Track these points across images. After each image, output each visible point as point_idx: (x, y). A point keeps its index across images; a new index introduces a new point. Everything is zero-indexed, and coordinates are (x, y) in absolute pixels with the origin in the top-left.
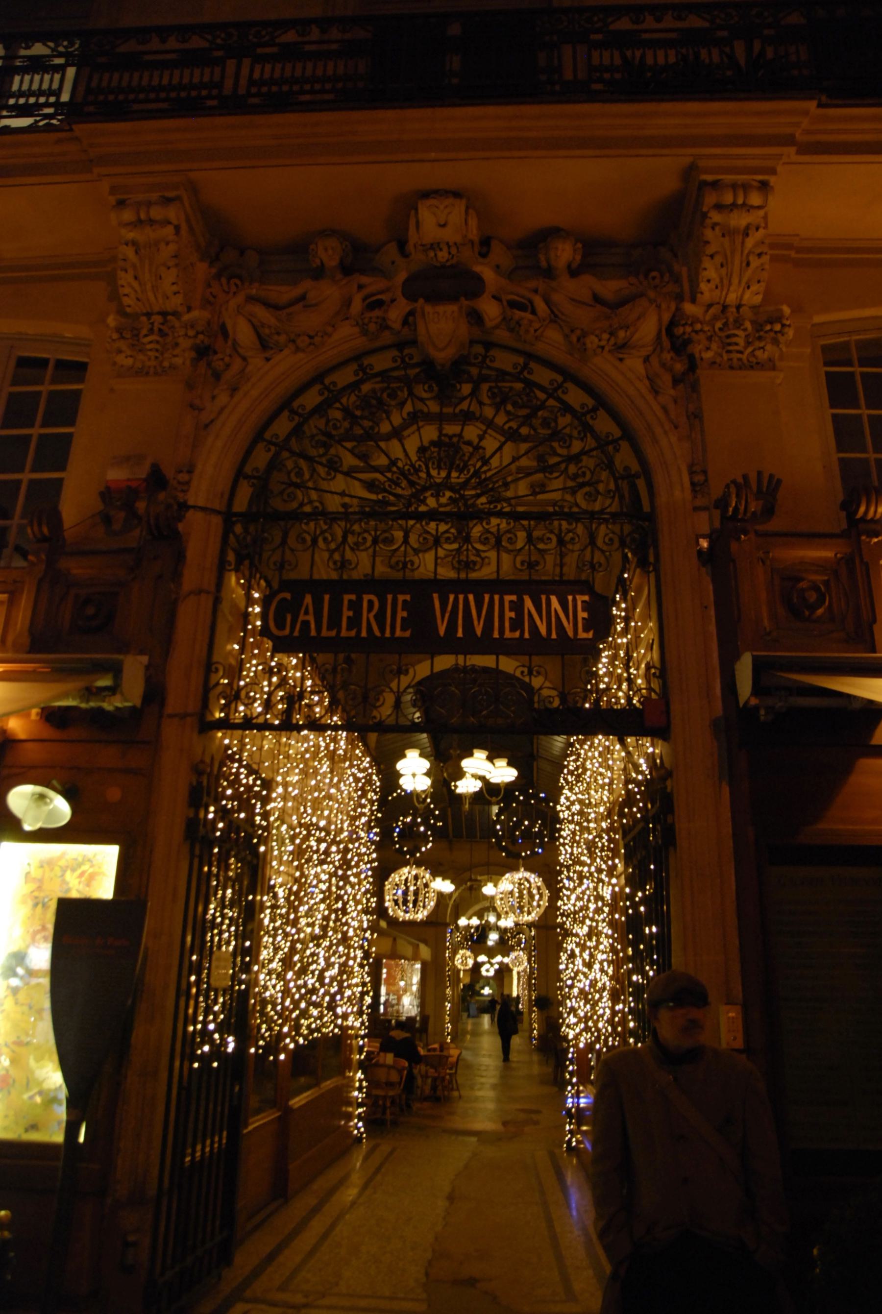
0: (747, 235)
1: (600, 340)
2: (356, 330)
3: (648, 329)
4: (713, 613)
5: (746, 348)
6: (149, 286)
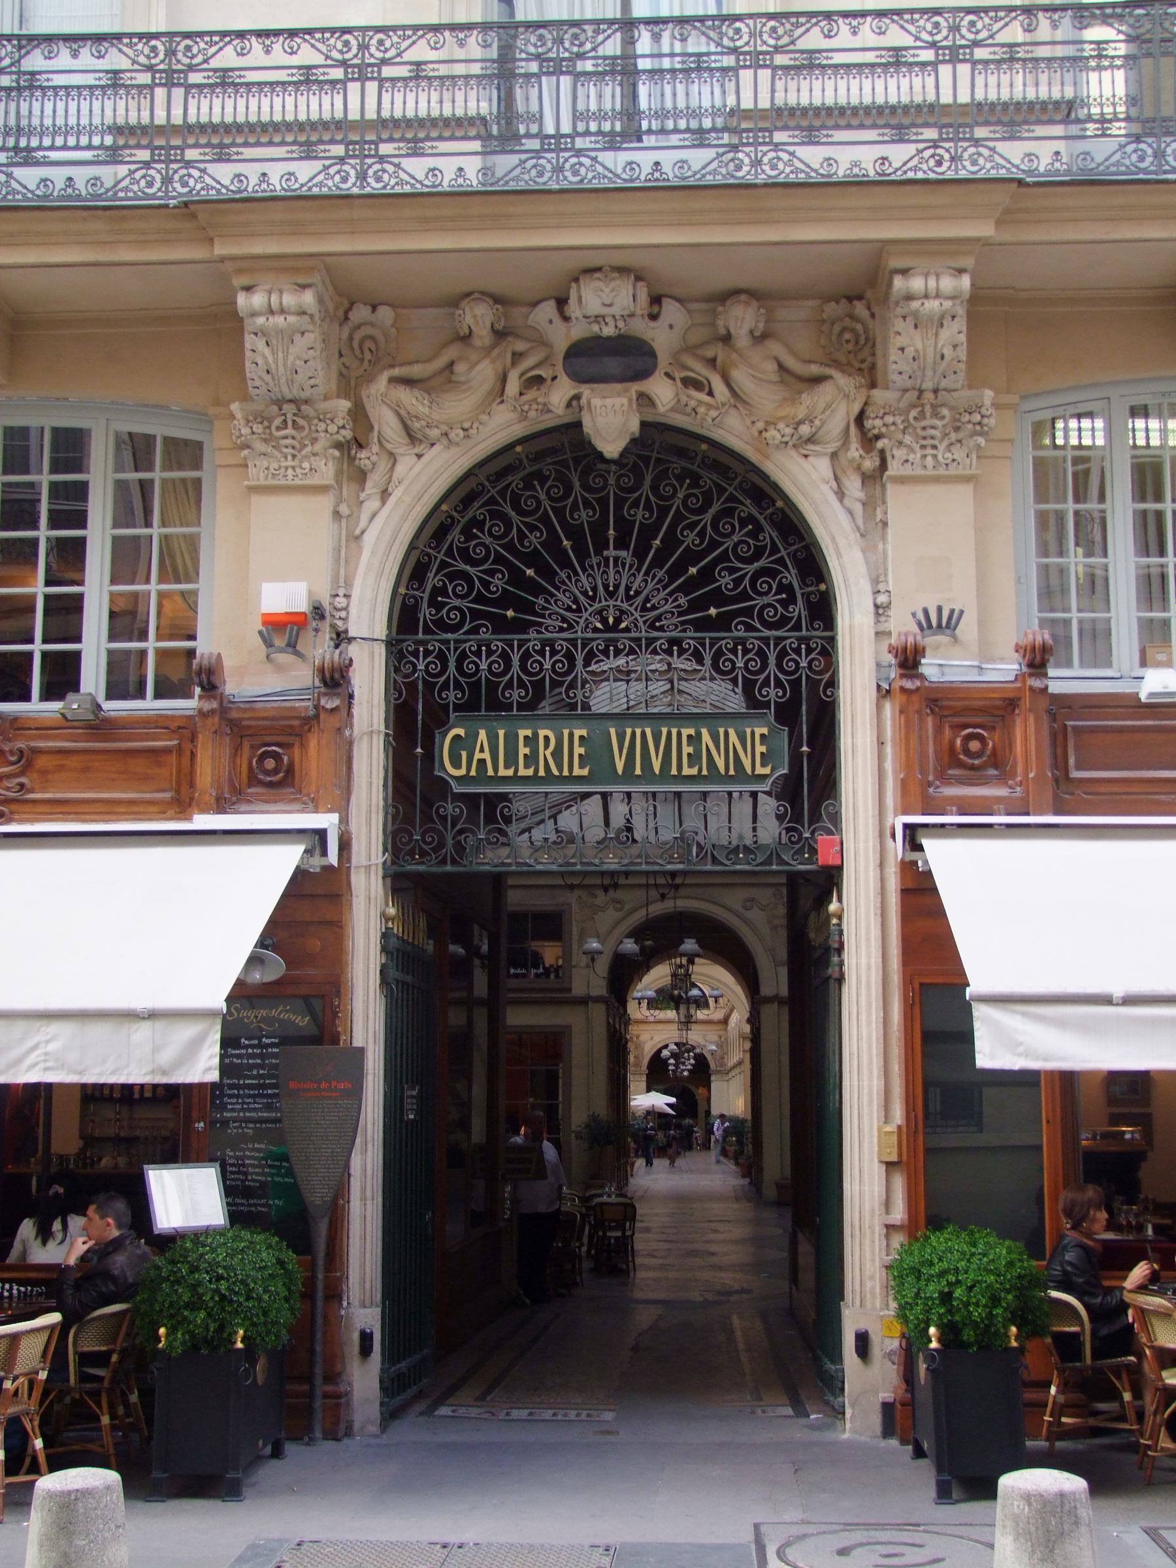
0: (942, 325)
3: (839, 418)
6: (283, 380)
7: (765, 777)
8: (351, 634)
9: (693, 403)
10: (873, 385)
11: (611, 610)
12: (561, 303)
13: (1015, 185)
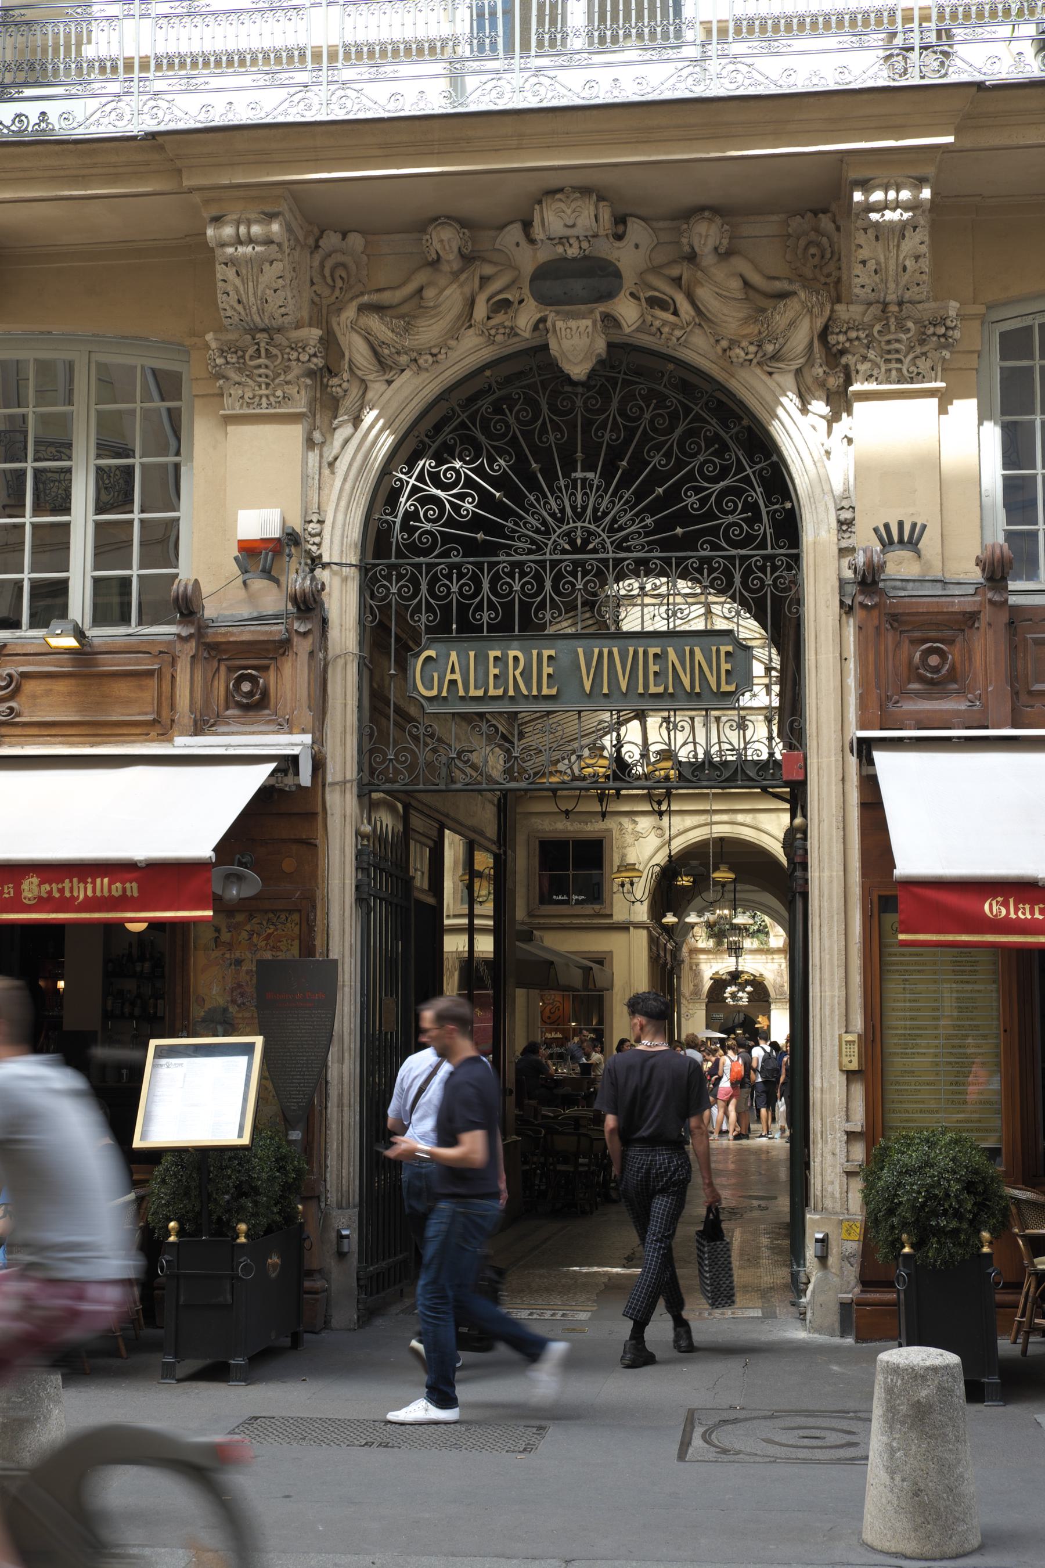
1: (747, 354)
2: (481, 340)
3: (801, 337)
4: (852, 666)
5: (908, 353)
8: (326, 559)
9: (657, 323)
10: (838, 300)
11: (579, 532)
12: (527, 225)
13: (975, 89)
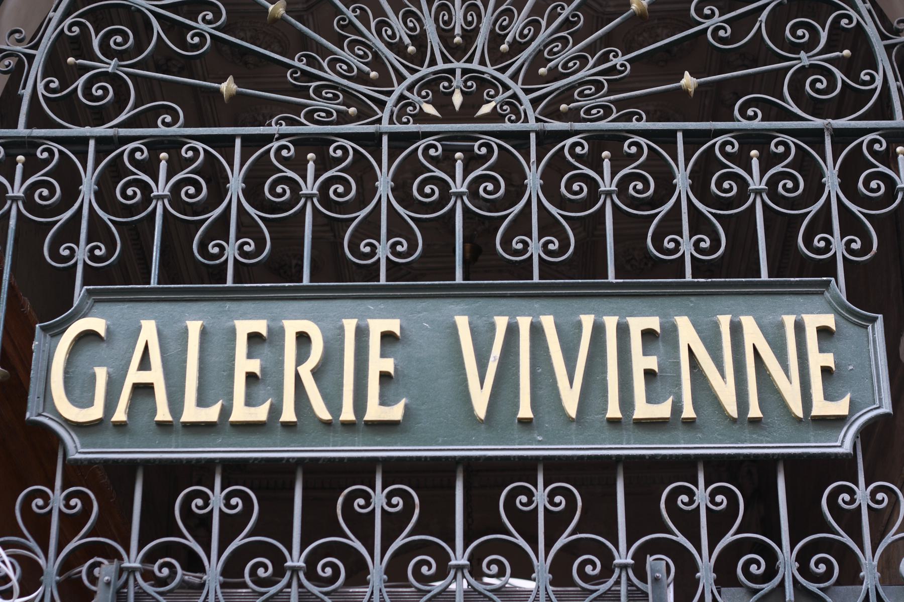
7: (838, 421)
11: (458, 81)
